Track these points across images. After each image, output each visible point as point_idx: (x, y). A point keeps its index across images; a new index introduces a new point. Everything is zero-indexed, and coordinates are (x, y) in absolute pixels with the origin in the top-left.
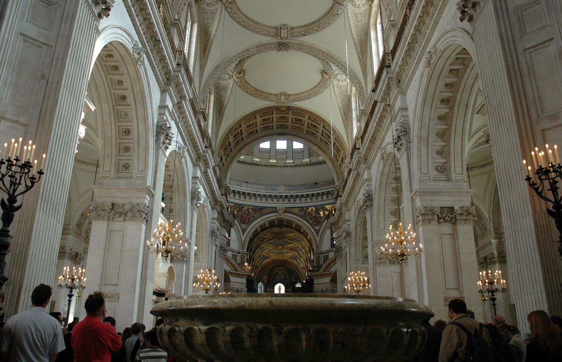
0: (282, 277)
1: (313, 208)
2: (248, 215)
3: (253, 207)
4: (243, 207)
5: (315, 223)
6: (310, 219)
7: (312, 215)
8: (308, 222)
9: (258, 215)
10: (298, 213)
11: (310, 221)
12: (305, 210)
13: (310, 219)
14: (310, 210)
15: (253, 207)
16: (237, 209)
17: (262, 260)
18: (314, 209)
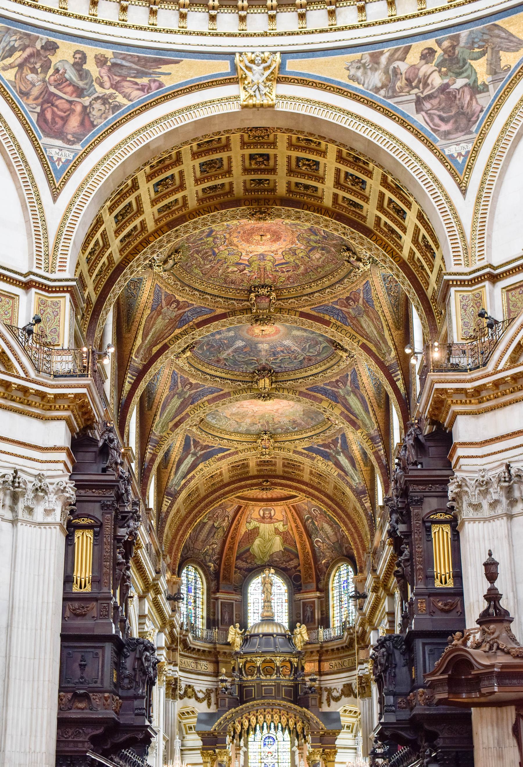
0: (277, 545)
1: (431, 43)
2: (80, 92)
3: (109, 53)
4: (52, 47)
5: (444, 127)
6: (419, 102)
8: (403, 123)
9: (135, 93)
10: (352, 78)
12: (391, 60)
13: (418, 110)
15: (109, 53)
16: (18, 57)
17: (189, 460)
18: (439, 52)
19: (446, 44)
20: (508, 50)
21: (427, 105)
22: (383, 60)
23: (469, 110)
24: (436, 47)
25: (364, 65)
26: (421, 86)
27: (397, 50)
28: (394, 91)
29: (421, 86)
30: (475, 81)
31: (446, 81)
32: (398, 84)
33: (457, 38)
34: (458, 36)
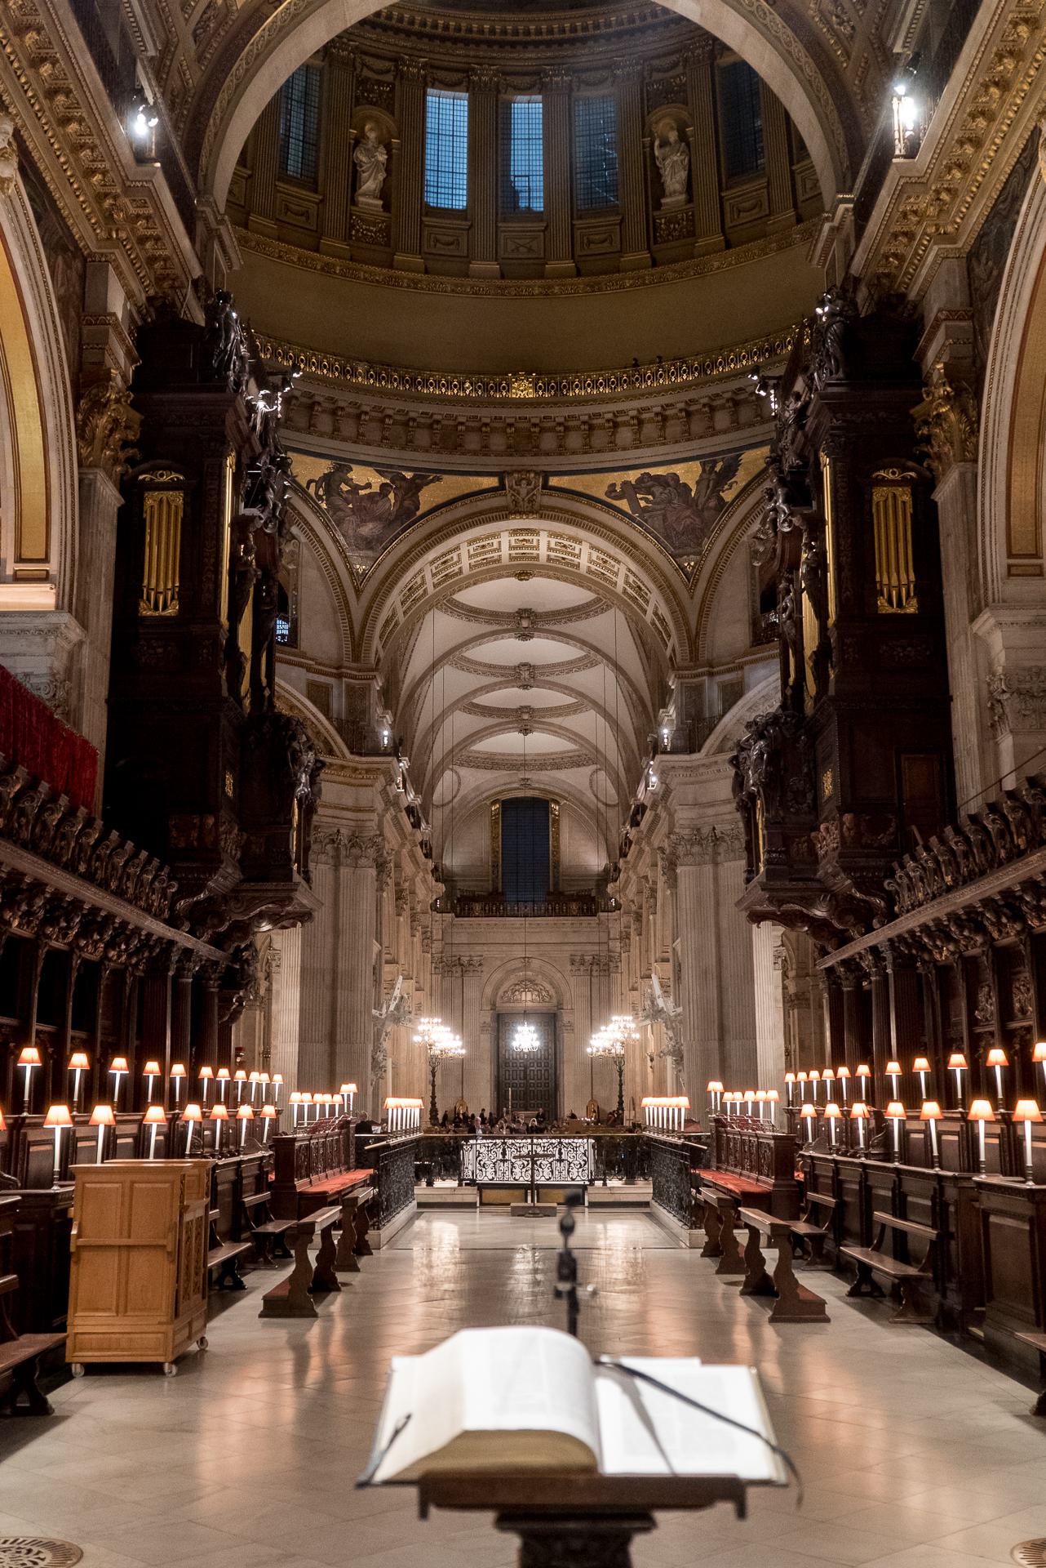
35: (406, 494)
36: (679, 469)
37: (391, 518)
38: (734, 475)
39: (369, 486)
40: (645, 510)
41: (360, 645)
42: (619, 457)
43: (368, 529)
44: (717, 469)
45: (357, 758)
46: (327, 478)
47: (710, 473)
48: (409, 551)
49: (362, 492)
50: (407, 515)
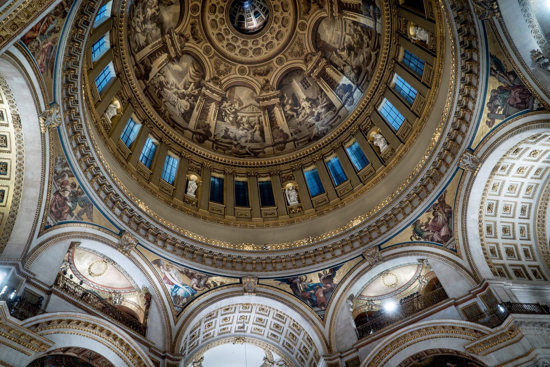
5: (53, 209)
6: (57, 192)
7: (65, 190)
11: (52, 196)
12: (67, 171)
13: (55, 194)
14: (70, 180)
18: (76, 189)
19: (80, 190)
20: (87, 215)
21: (57, 197)
22: (67, 168)
23: (63, 214)
24: (77, 187)
25: (63, 161)
26: (63, 189)
27: (72, 172)
28: (57, 179)
29: (63, 189)
30: (73, 210)
31: (68, 198)
32: (60, 180)
33: (83, 193)
34: (84, 193)
35: (443, 208)
36: (490, 88)
37: (447, 220)
38: (500, 61)
39: (429, 219)
40: (504, 113)
41: (476, 275)
42: (476, 112)
43: (443, 232)
44: (495, 69)
45: (498, 328)
46: (415, 231)
47: (496, 73)
48: (462, 224)
49: (430, 223)
50: (450, 215)
